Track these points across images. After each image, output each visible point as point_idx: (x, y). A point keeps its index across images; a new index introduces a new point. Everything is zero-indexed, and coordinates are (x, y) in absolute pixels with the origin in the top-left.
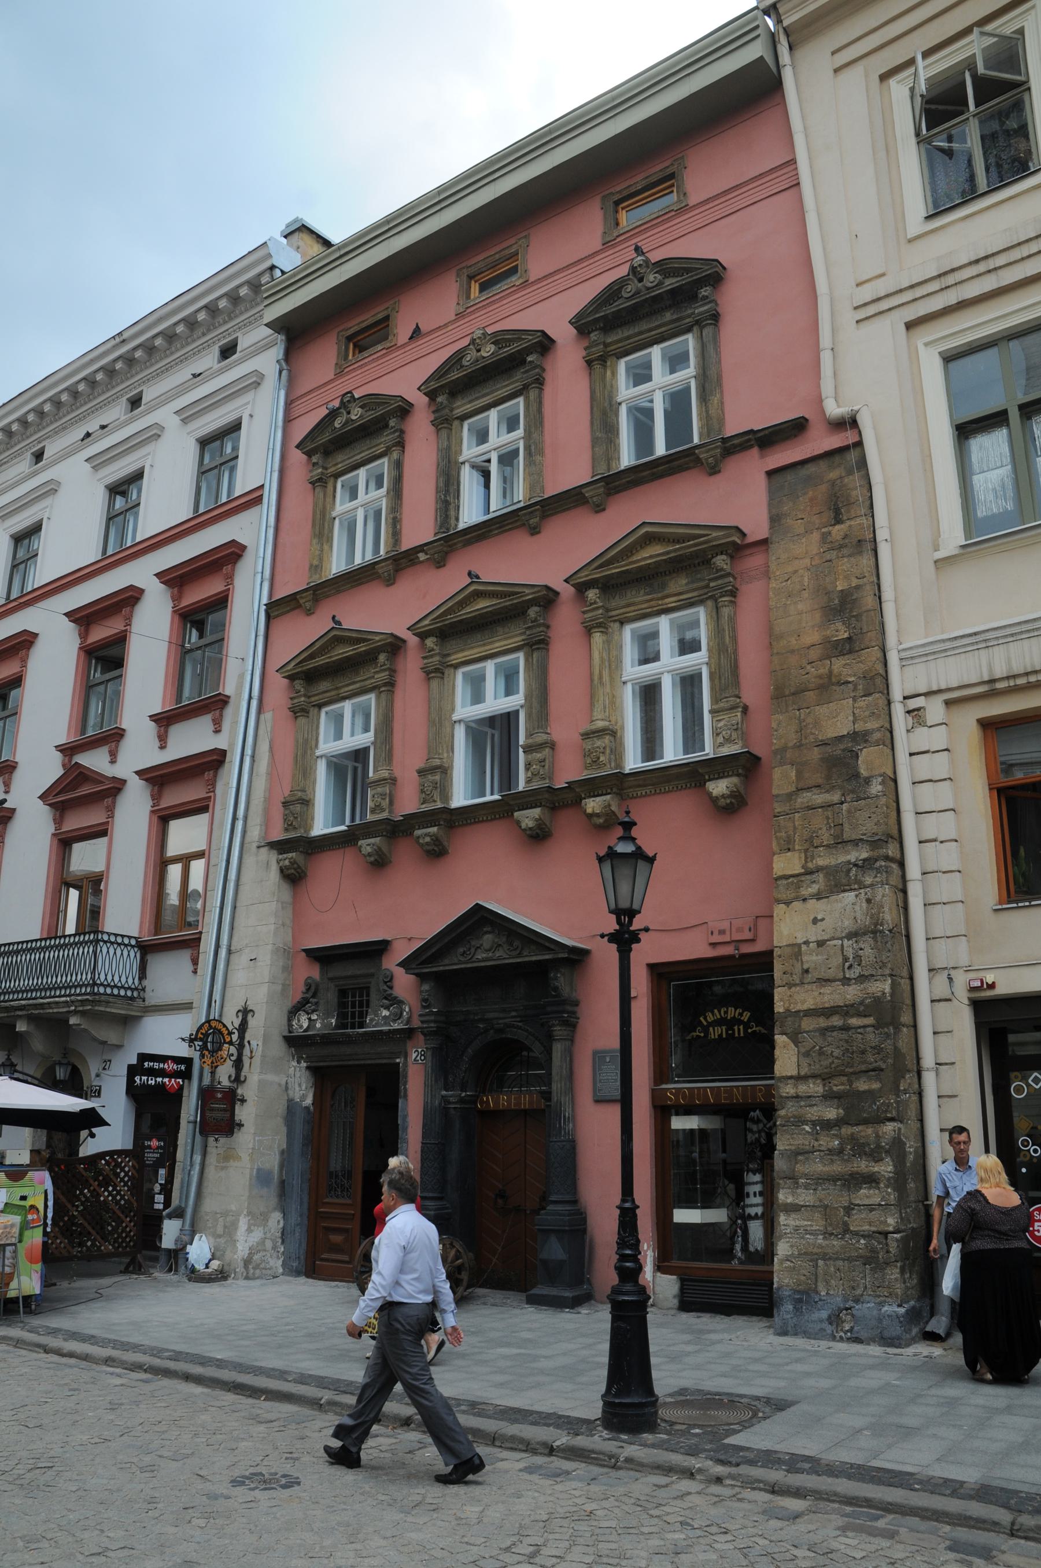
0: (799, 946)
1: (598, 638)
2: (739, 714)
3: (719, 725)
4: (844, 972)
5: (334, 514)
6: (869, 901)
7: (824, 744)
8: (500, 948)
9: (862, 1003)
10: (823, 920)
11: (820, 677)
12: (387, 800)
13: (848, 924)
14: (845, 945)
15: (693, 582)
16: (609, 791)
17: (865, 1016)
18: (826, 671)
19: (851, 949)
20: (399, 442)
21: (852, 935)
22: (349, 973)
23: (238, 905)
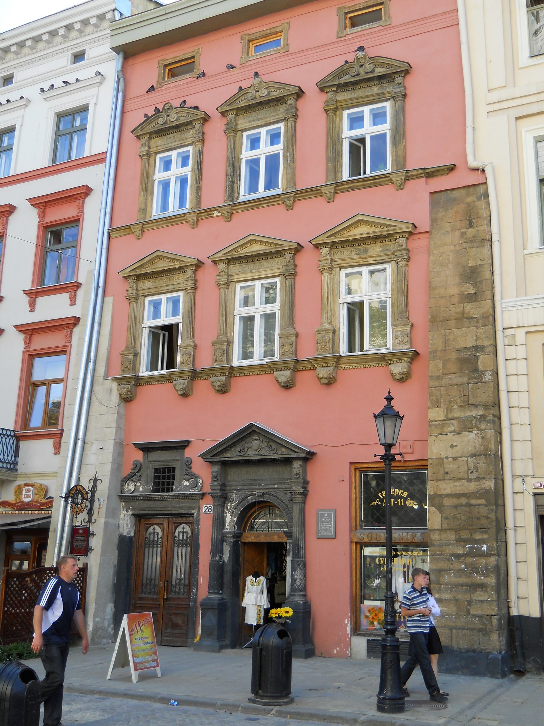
0: (442, 459)
1: (326, 275)
2: (409, 329)
3: (397, 334)
4: (468, 475)
5: (155, 178)
6: (483, 438)
7: (459, 350)
8: (263, 449)
9: (478, 492)
10: (456, 446)
11: (457, 313)
12: (192, 358)
13: (471, 449)
14: (469, 461)
15: (384, 250)
16: (332, 365)
17: (480, 499)
18: (462, 309)
19: (472, 463)
20: (201, 140)
21: (473, 455)
22: (163, 459)
23: (90, 415)
